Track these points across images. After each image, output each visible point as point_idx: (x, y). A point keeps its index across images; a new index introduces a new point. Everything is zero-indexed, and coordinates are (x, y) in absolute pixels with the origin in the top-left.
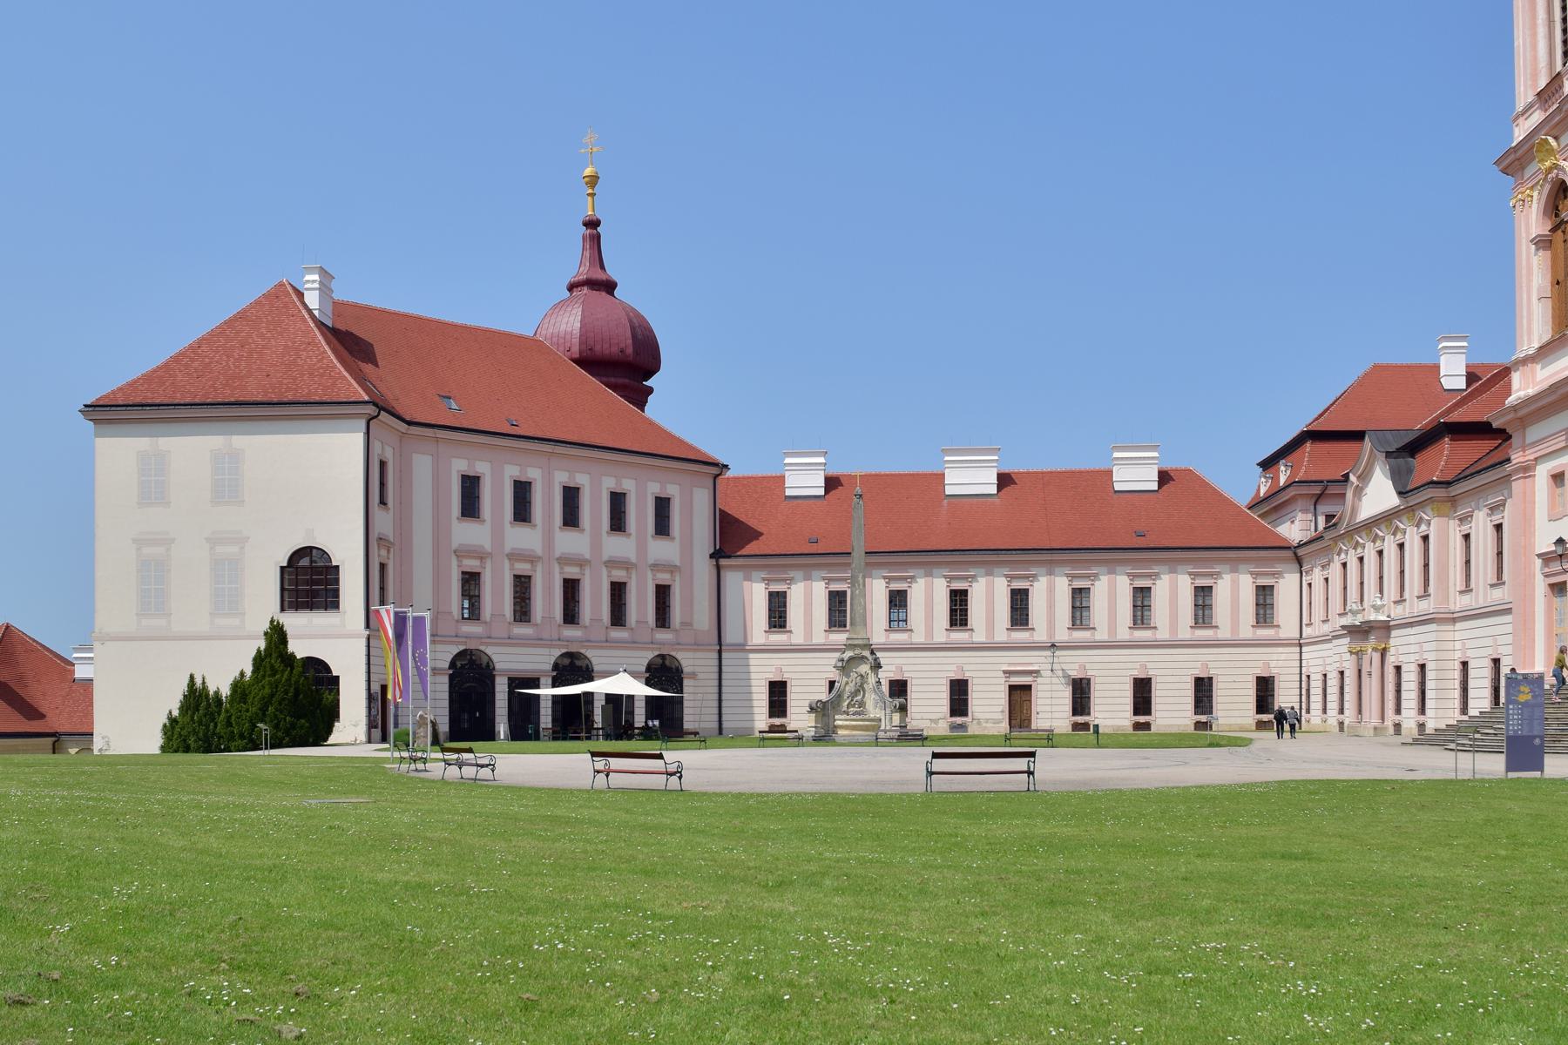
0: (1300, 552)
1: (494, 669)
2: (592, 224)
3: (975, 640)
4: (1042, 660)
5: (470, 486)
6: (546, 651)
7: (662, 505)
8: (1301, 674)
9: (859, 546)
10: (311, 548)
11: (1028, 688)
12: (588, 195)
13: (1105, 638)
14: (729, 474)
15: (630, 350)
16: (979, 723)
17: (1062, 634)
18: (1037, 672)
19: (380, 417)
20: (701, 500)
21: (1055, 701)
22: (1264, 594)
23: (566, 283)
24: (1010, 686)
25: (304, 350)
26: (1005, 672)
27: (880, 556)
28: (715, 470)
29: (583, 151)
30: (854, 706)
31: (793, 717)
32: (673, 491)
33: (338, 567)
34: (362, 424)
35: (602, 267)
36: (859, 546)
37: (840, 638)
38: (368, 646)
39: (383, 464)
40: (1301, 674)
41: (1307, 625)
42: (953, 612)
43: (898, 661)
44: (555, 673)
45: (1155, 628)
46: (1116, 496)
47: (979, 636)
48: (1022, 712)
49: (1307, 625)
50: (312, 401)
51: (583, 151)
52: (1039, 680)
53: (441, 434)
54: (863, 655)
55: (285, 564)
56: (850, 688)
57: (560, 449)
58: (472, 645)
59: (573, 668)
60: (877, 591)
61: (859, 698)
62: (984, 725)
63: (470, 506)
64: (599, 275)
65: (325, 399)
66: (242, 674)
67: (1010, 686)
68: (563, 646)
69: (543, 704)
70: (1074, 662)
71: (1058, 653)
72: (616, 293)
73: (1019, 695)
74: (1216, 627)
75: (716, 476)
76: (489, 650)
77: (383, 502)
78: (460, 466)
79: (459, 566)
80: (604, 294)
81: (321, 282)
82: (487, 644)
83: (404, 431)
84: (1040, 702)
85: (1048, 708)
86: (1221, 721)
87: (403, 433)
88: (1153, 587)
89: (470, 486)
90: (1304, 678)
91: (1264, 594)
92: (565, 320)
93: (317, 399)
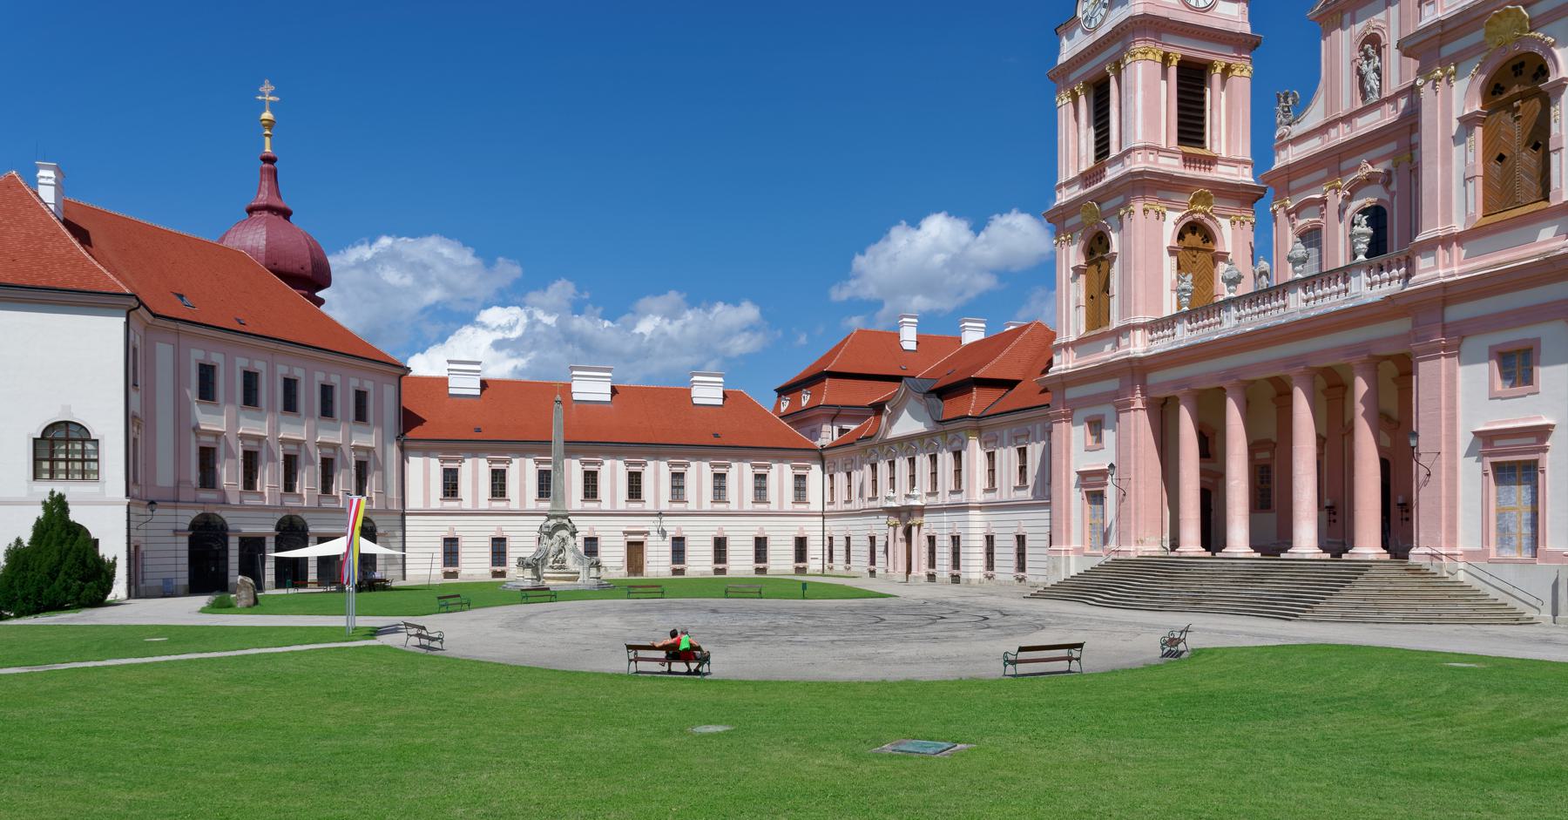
0: (825, 453)
1: (227, 530)
2: (269, 160)
3: (603, 508)
4: (652, 524)
5: (207, 375)
6: (270, 514)
7: (361, 397)
8: (823, 535)
9: (558, 437)
10: (67, 423)
11: (641, 543)
12: (267, 135)
13: (695, 508)
14: (411, 374)
15: (309, 268)
16: (606, 570)
17: (665, 506)
18: (647, 533)
19: (139, 310)
20: (390, 391)
21: (660, 554)
22: (800, 480)
23: (246, 206)
24: (628, 543)
25: (50, 240)
26: (624, 532)
27: (574, 447)
28: (399, 371)
29: (260, 98)
30: (558, 562)
31: (464, 566)
32: (368, 386)
33: (97, 441)
34: (124, 312)
35: (279, 197)
36: (558, 437)
37: (546, 505)
38: (128, 513)
39: (135, 350)
40: (823, 535)
41: (829, 503)
42: (586, 487)
43: (591, 524)
44: (278, 533)
45: (729, 502)
46: (695, 407)
47: (606, 505)
48: (636, 561)
49: (829, 503)
50: (69, 288)
51: (260, 98)
52: (648, 538)
53: (182, 327)
54: (559, 523)
55: (39, 436)
56: (553, 549)
57: (283, 347)
58: (210, 509)
59: (293, 531)
60: (574, 470)
61: (561, 555)
62: (610, 571)
63: (207, 391)
64: (276, 203)
65: (83, 288)
66: (19, 541)
67: (628, 543)
68: (199, 508)
69: (310, 564)
70: (673, 526)
71: (664, 518)
72: (291, 218)
73: (635, 549)
74: (769, 503)
75: (401, 376)
76: (224, 514)
77: (135, 385)
78: (197, 355)
79: (197, 442)
80: (281, 217)
81: (56, 180)
82: (222, 509)
83: (150, 322)
84: (649, 554)
85: (656, 559)
86: (771, 568)
87: (148, 324)
88: (727, 474)
89: (207, 375)
90: (826, 538)
91: (800, 480)
92: (251, 237)
93: (74, 287)
